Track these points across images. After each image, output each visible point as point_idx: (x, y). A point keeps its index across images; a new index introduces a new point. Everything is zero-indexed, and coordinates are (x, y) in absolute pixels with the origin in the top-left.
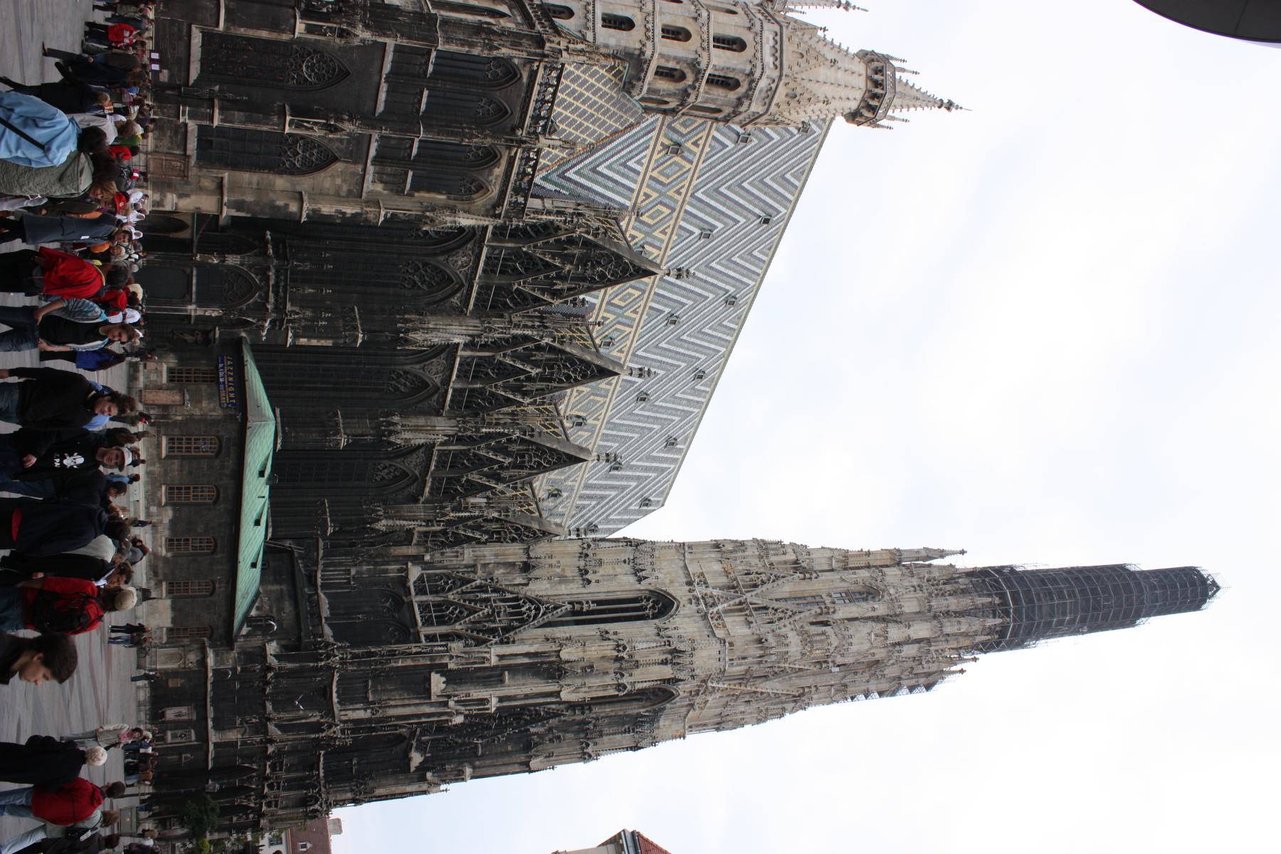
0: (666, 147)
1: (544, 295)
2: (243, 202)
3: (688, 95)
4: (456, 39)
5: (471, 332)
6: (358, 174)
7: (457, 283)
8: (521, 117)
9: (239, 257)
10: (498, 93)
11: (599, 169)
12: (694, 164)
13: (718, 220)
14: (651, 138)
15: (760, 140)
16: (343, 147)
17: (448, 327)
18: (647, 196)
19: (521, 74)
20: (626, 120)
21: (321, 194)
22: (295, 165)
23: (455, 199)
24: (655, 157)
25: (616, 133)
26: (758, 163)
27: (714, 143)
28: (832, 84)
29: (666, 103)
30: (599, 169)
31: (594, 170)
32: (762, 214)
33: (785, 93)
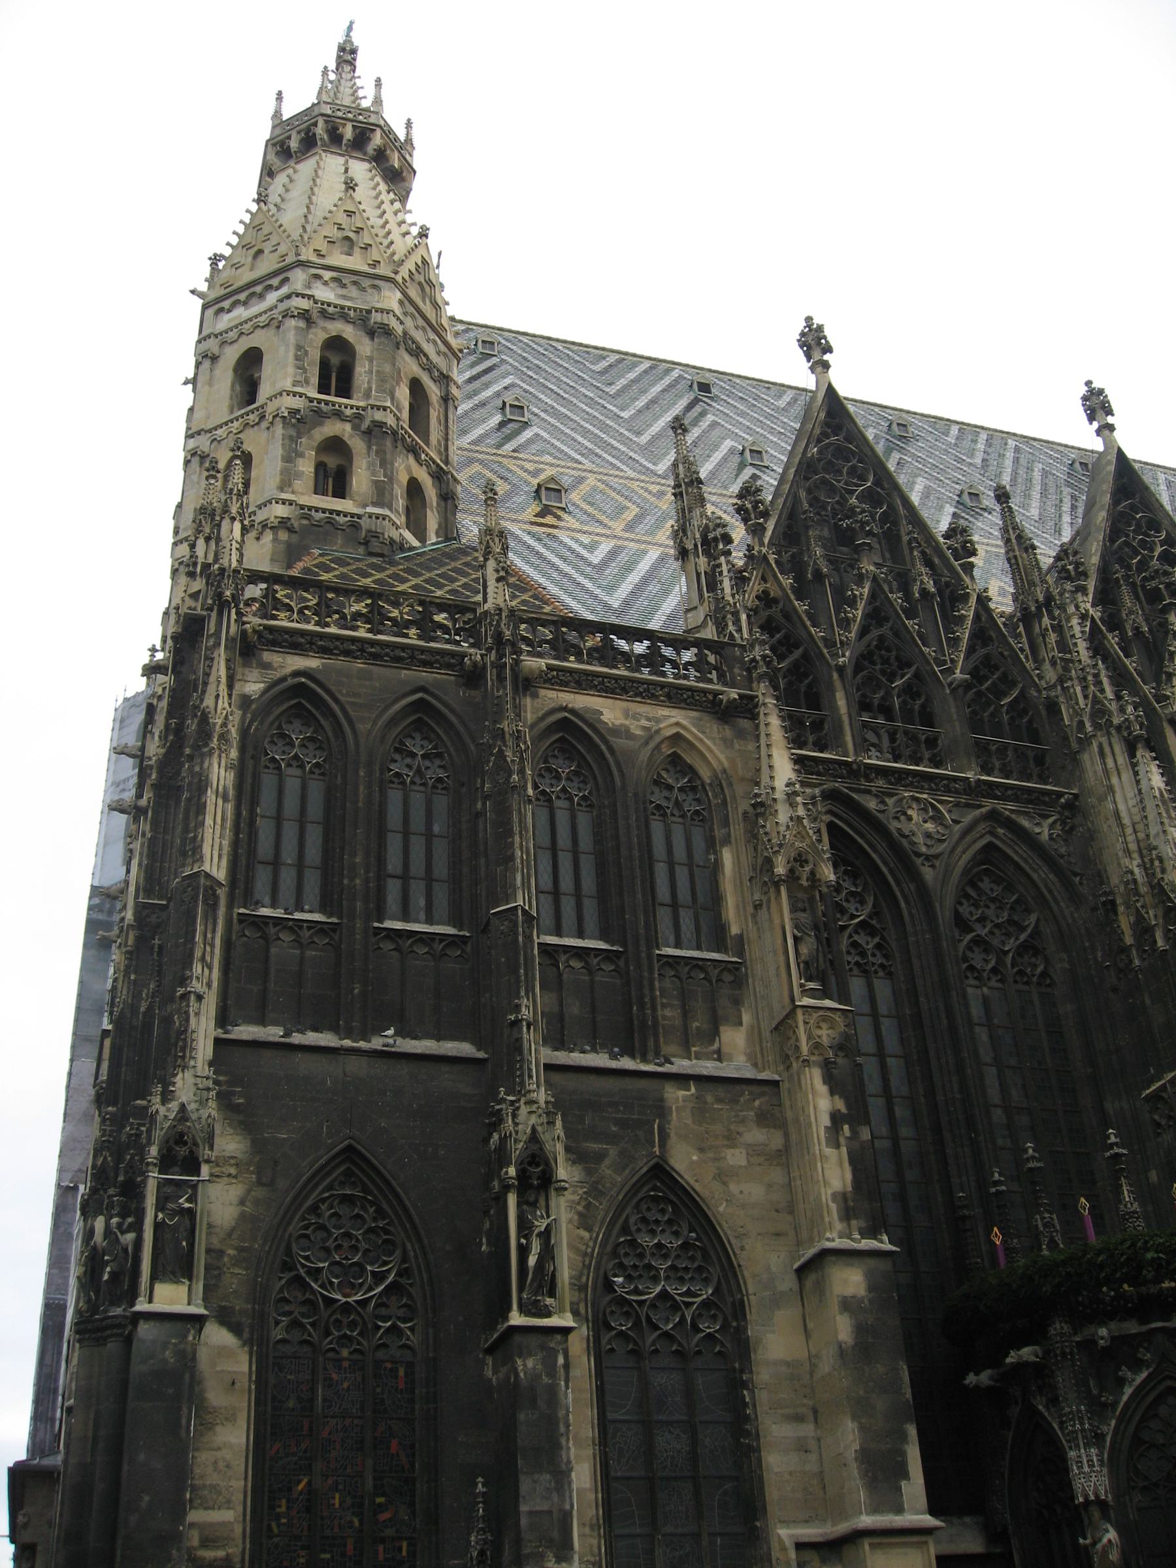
1: (962, 618)
2: (866, 1457)
3: (380, 425)
4: (186, 830)
5: (1122, 759)
6: (699, 1097)
7: (992, 833)
8: (425, 663)
9: (1072, 1454)
10: (362, 727)
16: (613, 1152)
17: (1126, 821)
19: (297, 674)
21: (791, 1209)
22: (706, 1304)
23: (726, 823)
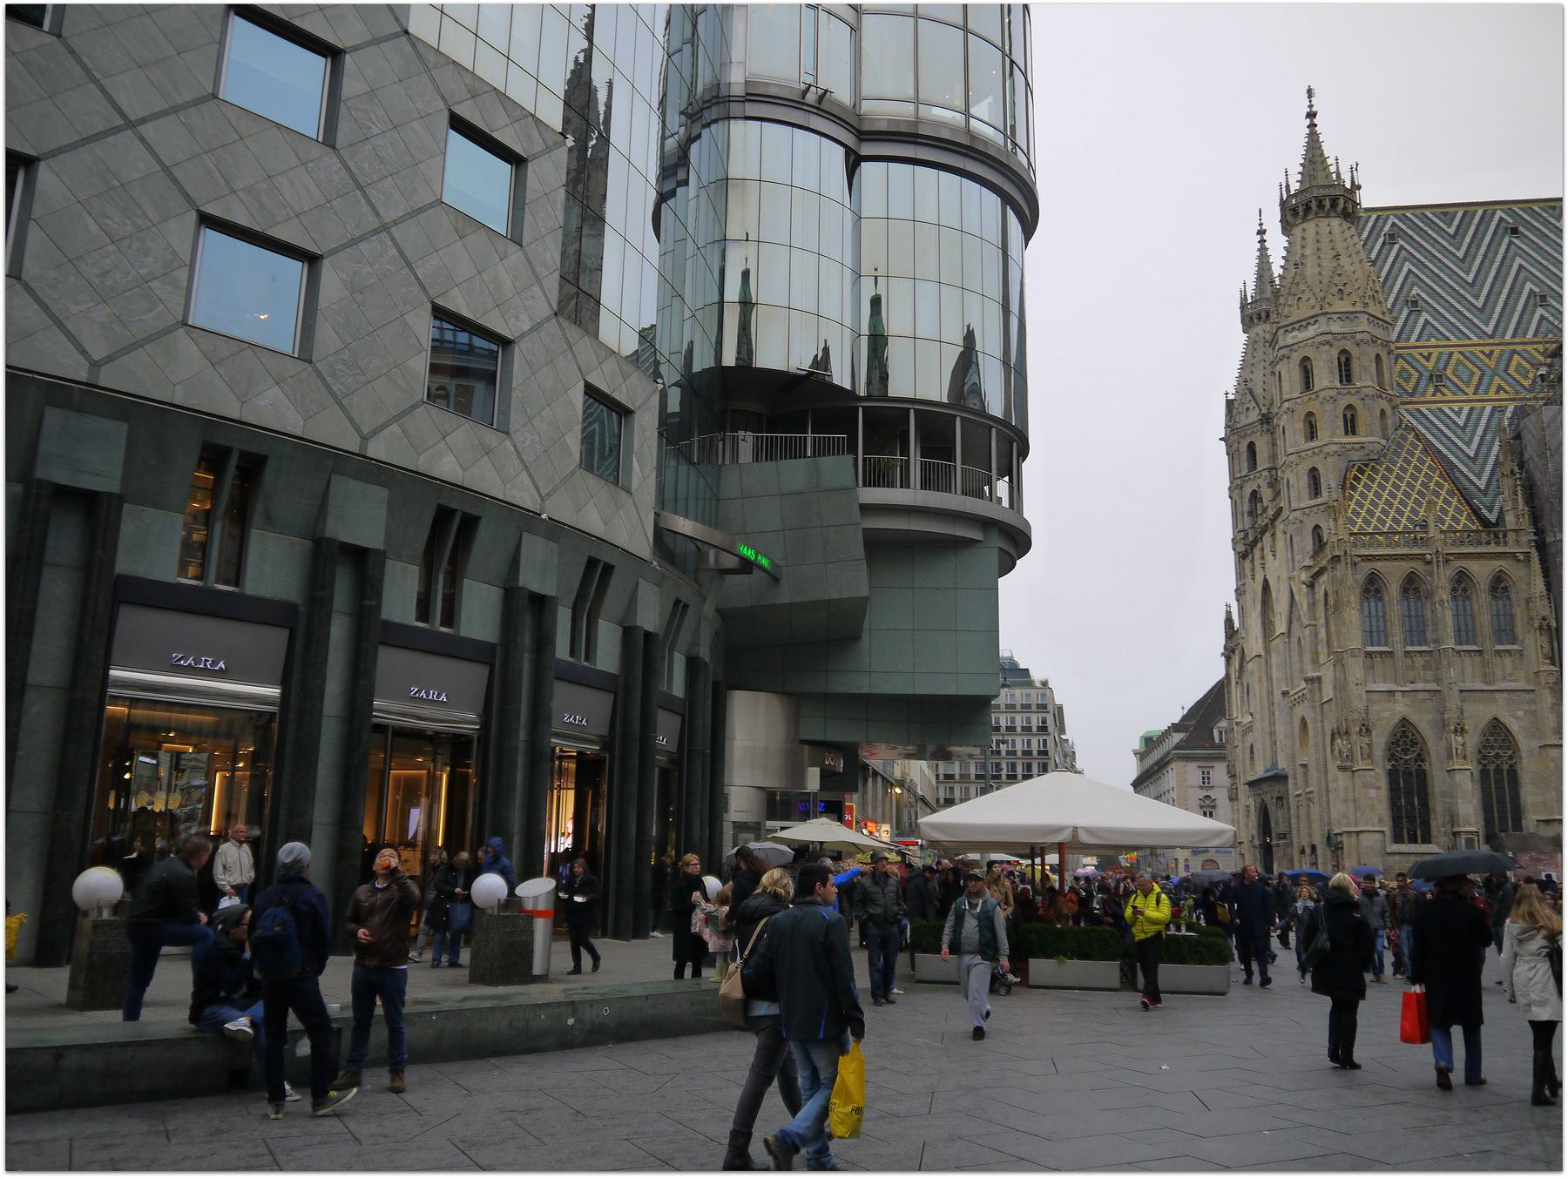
0: (1437, 389)
11: (1472, 454)
12: (1452, 349)
13: (1521, 292)
14: (1429, 410)
15: (1413, 284)
18: (1500, 388)
20: (1412, 444)
22: (1510, 756)
24: (1450, 397)
25: (1429, 449)
26: (1442, 275)
27: (1425, 337)
28: (1319, 257)
29: (1383, 412)
30: (1472, 454)
31: (1474, 460)
32: (1506, 240)
33: (1340, 302)
